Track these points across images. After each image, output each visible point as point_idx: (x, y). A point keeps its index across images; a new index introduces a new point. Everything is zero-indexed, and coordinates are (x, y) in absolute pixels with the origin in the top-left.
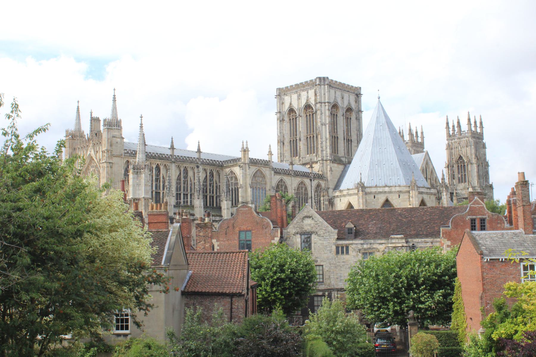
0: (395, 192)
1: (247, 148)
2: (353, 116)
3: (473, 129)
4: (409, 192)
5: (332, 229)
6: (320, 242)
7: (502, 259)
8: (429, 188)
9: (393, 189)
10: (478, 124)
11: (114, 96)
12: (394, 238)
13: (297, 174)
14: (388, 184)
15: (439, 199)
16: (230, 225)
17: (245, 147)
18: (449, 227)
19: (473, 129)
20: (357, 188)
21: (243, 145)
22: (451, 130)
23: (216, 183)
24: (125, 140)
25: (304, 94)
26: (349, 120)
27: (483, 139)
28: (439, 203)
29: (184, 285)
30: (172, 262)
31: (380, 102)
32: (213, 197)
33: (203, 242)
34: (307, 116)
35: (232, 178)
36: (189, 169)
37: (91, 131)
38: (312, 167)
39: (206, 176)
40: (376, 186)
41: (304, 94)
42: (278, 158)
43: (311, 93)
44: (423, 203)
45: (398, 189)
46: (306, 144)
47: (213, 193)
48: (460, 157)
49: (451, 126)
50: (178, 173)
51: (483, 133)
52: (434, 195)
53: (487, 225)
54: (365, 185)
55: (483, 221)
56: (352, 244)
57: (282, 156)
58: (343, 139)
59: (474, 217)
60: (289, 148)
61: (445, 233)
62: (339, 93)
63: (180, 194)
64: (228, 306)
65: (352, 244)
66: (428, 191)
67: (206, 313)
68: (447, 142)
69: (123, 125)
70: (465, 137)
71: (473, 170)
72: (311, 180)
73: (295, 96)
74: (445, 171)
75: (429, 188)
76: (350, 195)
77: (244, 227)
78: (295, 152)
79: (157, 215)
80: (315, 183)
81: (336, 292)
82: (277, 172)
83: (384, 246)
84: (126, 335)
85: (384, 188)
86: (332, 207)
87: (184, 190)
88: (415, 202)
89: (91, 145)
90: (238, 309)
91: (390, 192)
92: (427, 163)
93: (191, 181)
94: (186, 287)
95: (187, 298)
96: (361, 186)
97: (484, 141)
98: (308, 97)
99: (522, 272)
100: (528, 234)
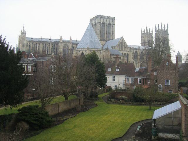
51: (168, 29)
62: (105, 20)
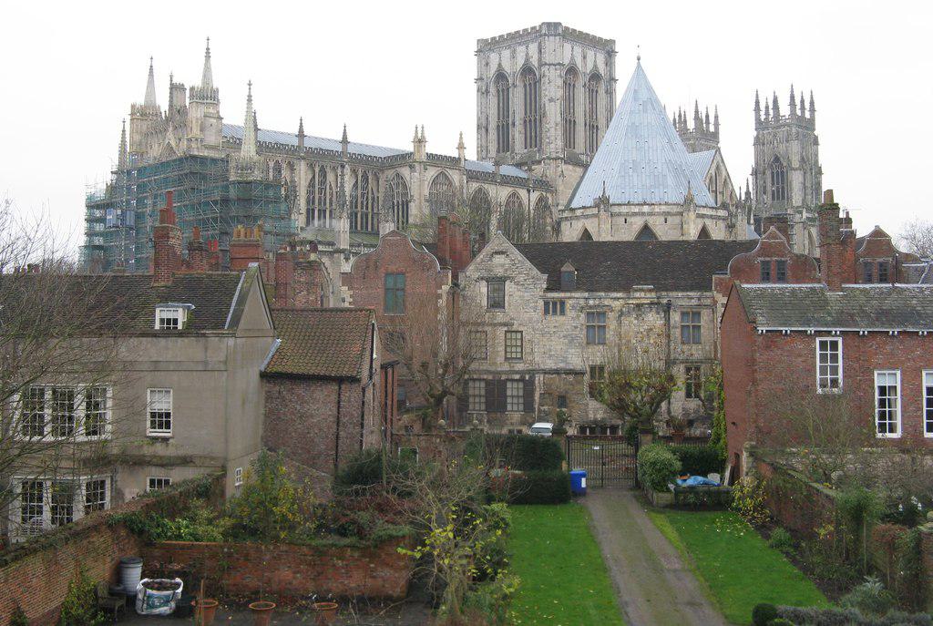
0: (659, 214)
1: (423, 136)
2: (602, 91)
3: (799, 113)
4: (681, 214)
5: (539, 273)
6: (519, 293)
7: (786, 331)
8: (716, 208)
9: (657, 209)
10: (807, 105)
11: (208, 49)
12: (636, 291)
13: (506, 181)
14: (648, 201)
15: (731, 227)
16: (371, 264)
17: (419, 135)
18: (726, 274)
19: (799, 113)
20: (597, 206)
21: (416, 132)
22: (762, 113)
23: (373, 194)
24: (223, 121)
25: (521, 50)
26: (594, 93)
27: (814, 130)
28: (731, 232)
29: (266, 362)
30: (242, 324)
31: (639, 65)
32: (367, 215)
33: (305, 293)
34: (525, 86)
35: (398, 184)
36: (328, 170)
37: (171, 106)
38: (530, 170)
39: (357, 182)
40: (629, 204)
41: (521, 50)
42: (478, 154)
43: (533, 48)
44: (704, 232)
45: (664, 208)
46: (523, 131)
47: (367, 208)
48: (777, 159)
49: (762, 107)
50: (310, 177)
52: (724, 220)
53: (789, 273)
54: (611, 202)
55: (781, 264)
56: (569, 298)
57: (483, 150)
58: (583, 120)
59: (768, 259)
60: (495, 137)
61: (720, 283)
62: (578, 50)
63: (313, 210)
64: (334, 397)
65: (569, 298)
66: (713, 213)
67: (298, 407)
68: (755, 133)
69: (221, 96)
70: (784, 126)
71: (796, 179)
72: (529, 191)
73: (506, 53)
74: (750, 178)
75: (716, 208)
76: (587, 217)
77: (392, 268)
78: (505, 144)
79: (246, 246)
80: (535, 196)
81: (542, 376)
82: (472, 175)
83: (622, 301)
84: (165, 440)
85: (641, 207)
86: (557, 236)
87: (320, 203)
88: (692, 233)
89: (171, 129)
90: (349, 401)
91: (651, 214)
92: (718, 168)
93: (331, 189)
94: (269, 364)
95: (269, 382)
96: (603, 202)
97: (816, 133)
98: (527, 54)
99: (818, 352)
100: (834, 291)
